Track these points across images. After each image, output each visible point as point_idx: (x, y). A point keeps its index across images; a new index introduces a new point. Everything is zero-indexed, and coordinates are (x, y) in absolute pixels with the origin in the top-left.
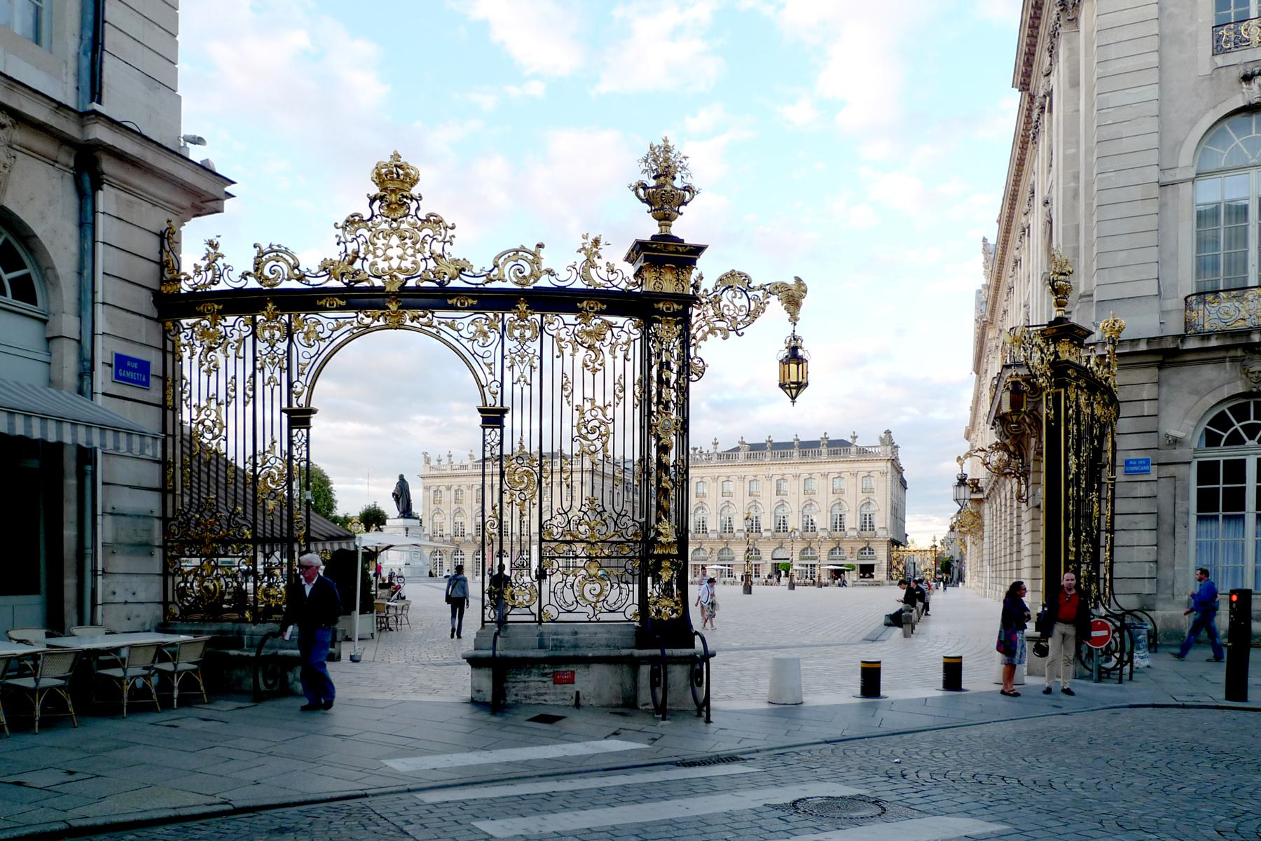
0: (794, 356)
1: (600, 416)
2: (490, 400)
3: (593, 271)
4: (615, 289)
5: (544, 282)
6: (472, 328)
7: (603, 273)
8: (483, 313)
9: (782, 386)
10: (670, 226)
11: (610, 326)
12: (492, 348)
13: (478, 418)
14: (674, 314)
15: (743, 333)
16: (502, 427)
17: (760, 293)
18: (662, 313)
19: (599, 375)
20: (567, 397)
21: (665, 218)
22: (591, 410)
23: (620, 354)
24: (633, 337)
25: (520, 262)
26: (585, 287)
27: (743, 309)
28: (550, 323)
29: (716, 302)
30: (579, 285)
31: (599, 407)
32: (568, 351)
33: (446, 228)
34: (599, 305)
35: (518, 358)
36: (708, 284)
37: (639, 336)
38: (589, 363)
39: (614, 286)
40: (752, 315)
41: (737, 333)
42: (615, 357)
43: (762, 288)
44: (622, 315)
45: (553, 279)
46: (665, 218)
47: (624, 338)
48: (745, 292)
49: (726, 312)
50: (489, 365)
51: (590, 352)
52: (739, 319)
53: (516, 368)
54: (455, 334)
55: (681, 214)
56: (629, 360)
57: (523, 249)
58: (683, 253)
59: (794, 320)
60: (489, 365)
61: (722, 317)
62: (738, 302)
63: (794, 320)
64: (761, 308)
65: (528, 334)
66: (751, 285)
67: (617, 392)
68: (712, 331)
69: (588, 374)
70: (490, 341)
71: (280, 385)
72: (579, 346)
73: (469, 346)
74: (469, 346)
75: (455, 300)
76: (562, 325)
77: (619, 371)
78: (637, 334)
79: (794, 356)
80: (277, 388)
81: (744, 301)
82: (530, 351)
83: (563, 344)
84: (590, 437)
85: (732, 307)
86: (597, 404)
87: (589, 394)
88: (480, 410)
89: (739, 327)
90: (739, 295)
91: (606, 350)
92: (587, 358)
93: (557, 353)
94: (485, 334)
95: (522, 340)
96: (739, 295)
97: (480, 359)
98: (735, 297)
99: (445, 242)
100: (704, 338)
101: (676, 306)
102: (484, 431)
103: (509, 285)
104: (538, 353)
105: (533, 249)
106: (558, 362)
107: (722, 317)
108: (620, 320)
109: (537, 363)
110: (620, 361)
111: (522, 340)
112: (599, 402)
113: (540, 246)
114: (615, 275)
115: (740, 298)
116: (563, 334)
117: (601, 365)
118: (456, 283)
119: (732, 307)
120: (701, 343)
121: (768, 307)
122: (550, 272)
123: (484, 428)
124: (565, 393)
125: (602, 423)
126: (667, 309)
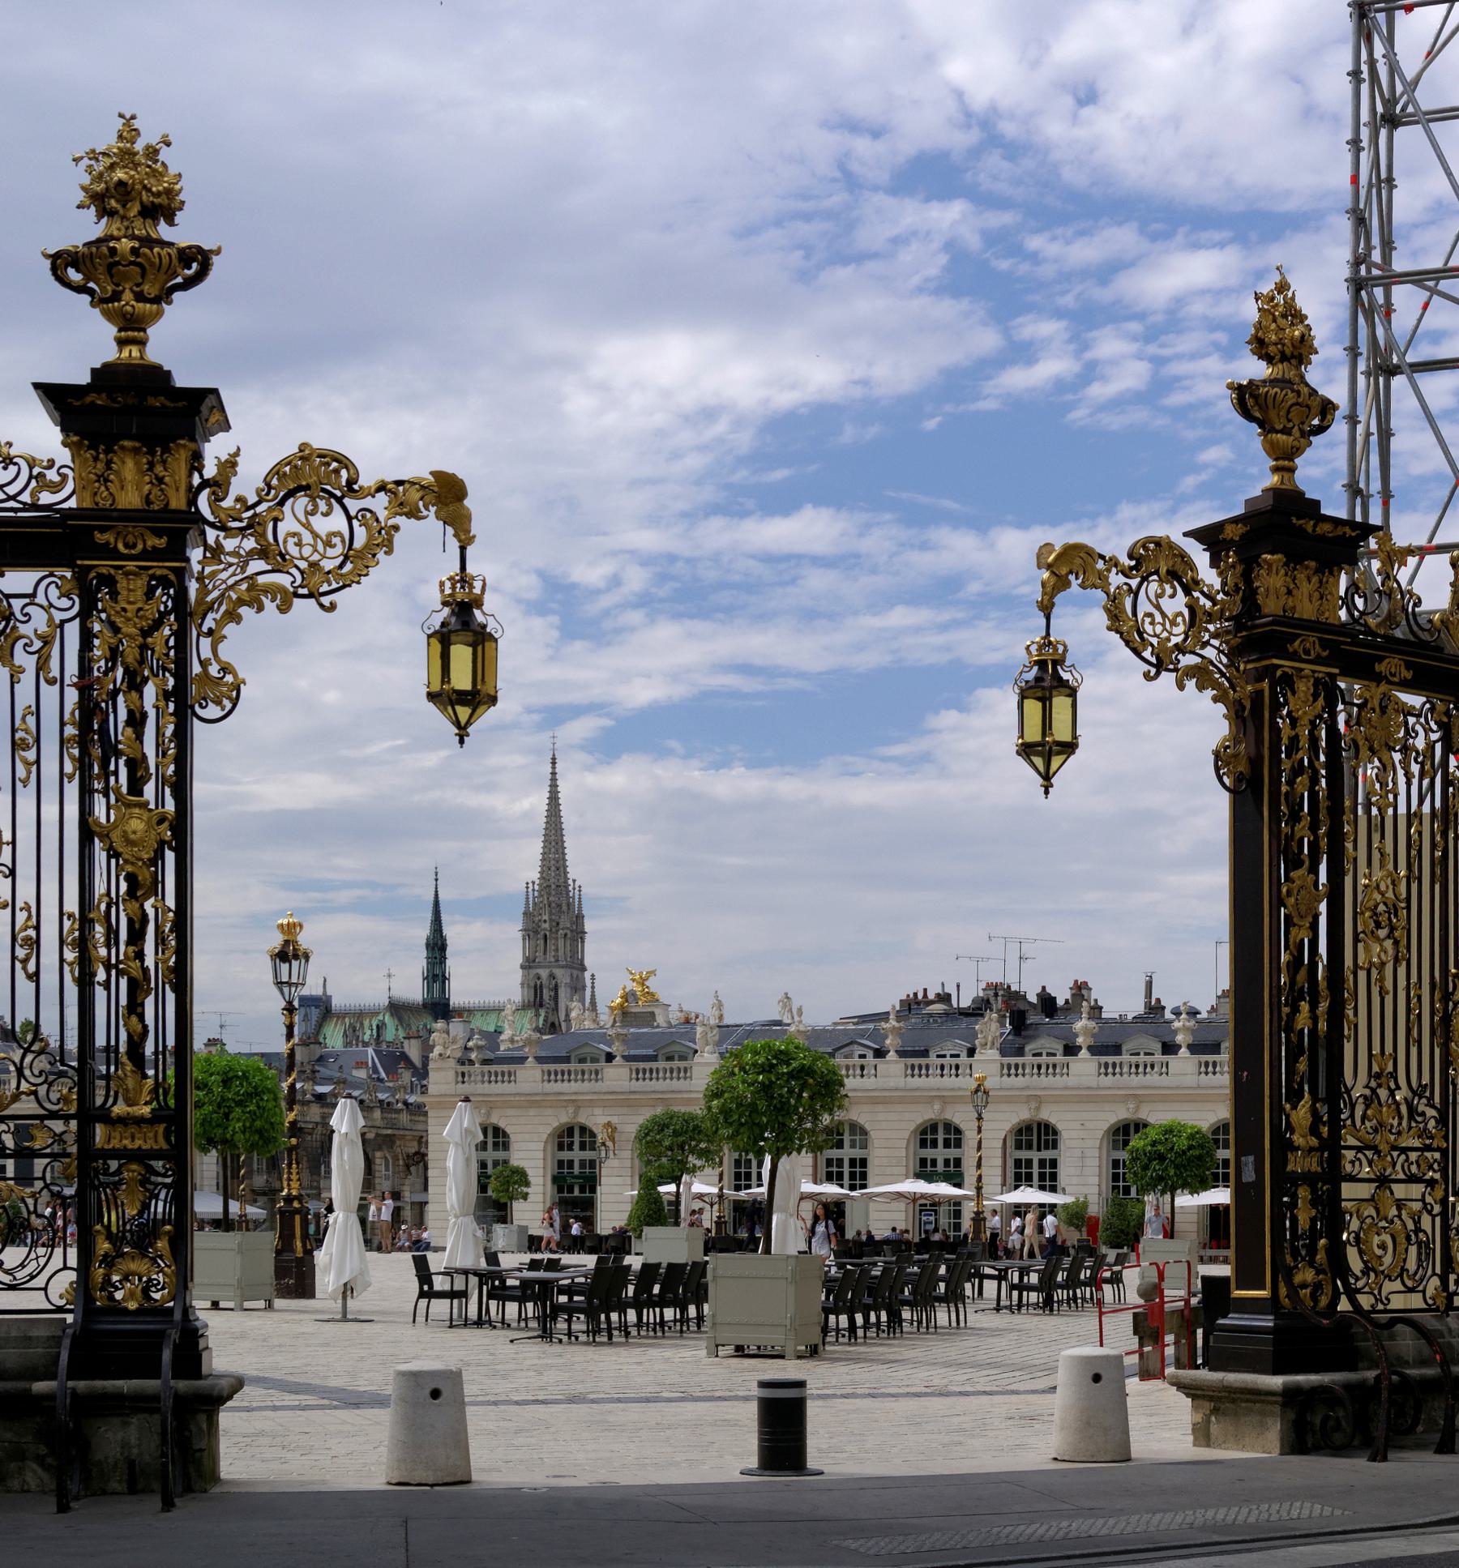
15: (332, 607)
24: (58, 616)
27: (336, 540)
37: (76, 608)
41: (322, 606)
46: (132, 329)
48: (340, 501)
49: (294, 551)
62: (322, 525)
64: (384, 539)
81: (338, 521)
85: (307, 537)
90: (322, 506)
96: (322, 506)
98: (313, 514)
107: (279, 560)
110: (28, 680)
114: (13, 469)
115: (326, 515)
119: (307, 537)
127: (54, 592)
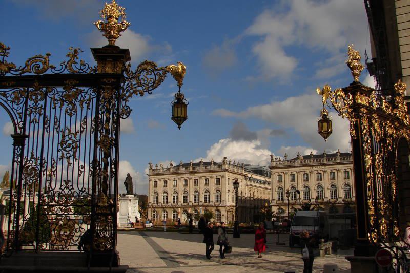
0: (179, 103)
1: (73, 138)
2: (19, 131)
3: (73, 65)
4: (84, 73)
5: (49, 72)
6: (13, 96)
7: (78, 66)
8: (19, 88)
9: (174, 118)
10: (115, 41)
11: (82, 91)
12: (21, 105)
13: (12, 141)
14: (112, 84)
15: (151, 93)
16: (23, 145)
17: (161, 72)
18: (105, 84)
19: (74, 117)
20: (57, 129)
21: (110, 37)
22: (68, 135)
23: (85, 105)
24: (92, 97)
25: (38, 63)
26: (69, 73)
28: (50, 92)
29: (136, 76)
30: (66, 72)
31: (73, 133)
32: (58, 105)
33: (6, 49)
34: (75, 81)
35: (33, 110)
36: (133, 69)
38: (69, 111)
39: (83, 72)
40: (156, 84)
42: (82, 108)
43: (162, 69)
44: (86, 86)
45: (53, 70)
47: (88, 97)
48: (153, 71)
49: (142, 82)
50: (19, 114)
51: (70, 105)
52: (150, 85)
53: (32, 115)
54: (5, 99)
55: (121, 35)
56: (89, 109)
57: (40, 57)
58: (116, 53)
59: (180, 85)
60: (19, 114)
61: (140, 84)
62: (149, 77)
63: (180, 85)
64: (161, 80)
65: (39, 97)
66: (156, 68)
67: (82, 125)
68: (135, 92)
69: (68, 117)
70: (21, 102)
71: (39, 123)
72: (64, 103)
73: (11, 105)
74: (11, 105)
75: (5, 83)
76: (56, 92)
77: (84, 114)
78: (94, 95)
79: (179, 103)
80: (37, 125)
81: (153, 76)
82: (40, 106)
83: (56, 102)
84: (68, 149)
85: (146, 79)
86: (71, 132)
87: (68, 125)
88: (12, 136)
89: (149, 89)
90: (149, 73)
91: (77, 104)
92: (68, 108)
93: (53, 106)
94: (19, 99)
95: (36, 101)
97: (15, 111)
98: (147, 74)
99: (4, 56)
100: (130, 96)
101: (113, 80)
102: (15, 147)
103: (32, 74)
104: (43, 107)
105: (45, 56)
106: (53, 111)
107: (140, 84)
108: (86, 89)
109: (42, 112)
111: (36, 101)
112: (73, 131)
113: (48, 55)
115: (150, 75)
116: (56, 97)
117: (74, 112)
118: (8, 75)
119: (146, 79)
120: (129, 99)
121: (165, 79)
122: (52, 67)
123: (14, 145)
124: (56, 127)
125: (74, 142)
126: (108, 81)
127: (91, 92)
